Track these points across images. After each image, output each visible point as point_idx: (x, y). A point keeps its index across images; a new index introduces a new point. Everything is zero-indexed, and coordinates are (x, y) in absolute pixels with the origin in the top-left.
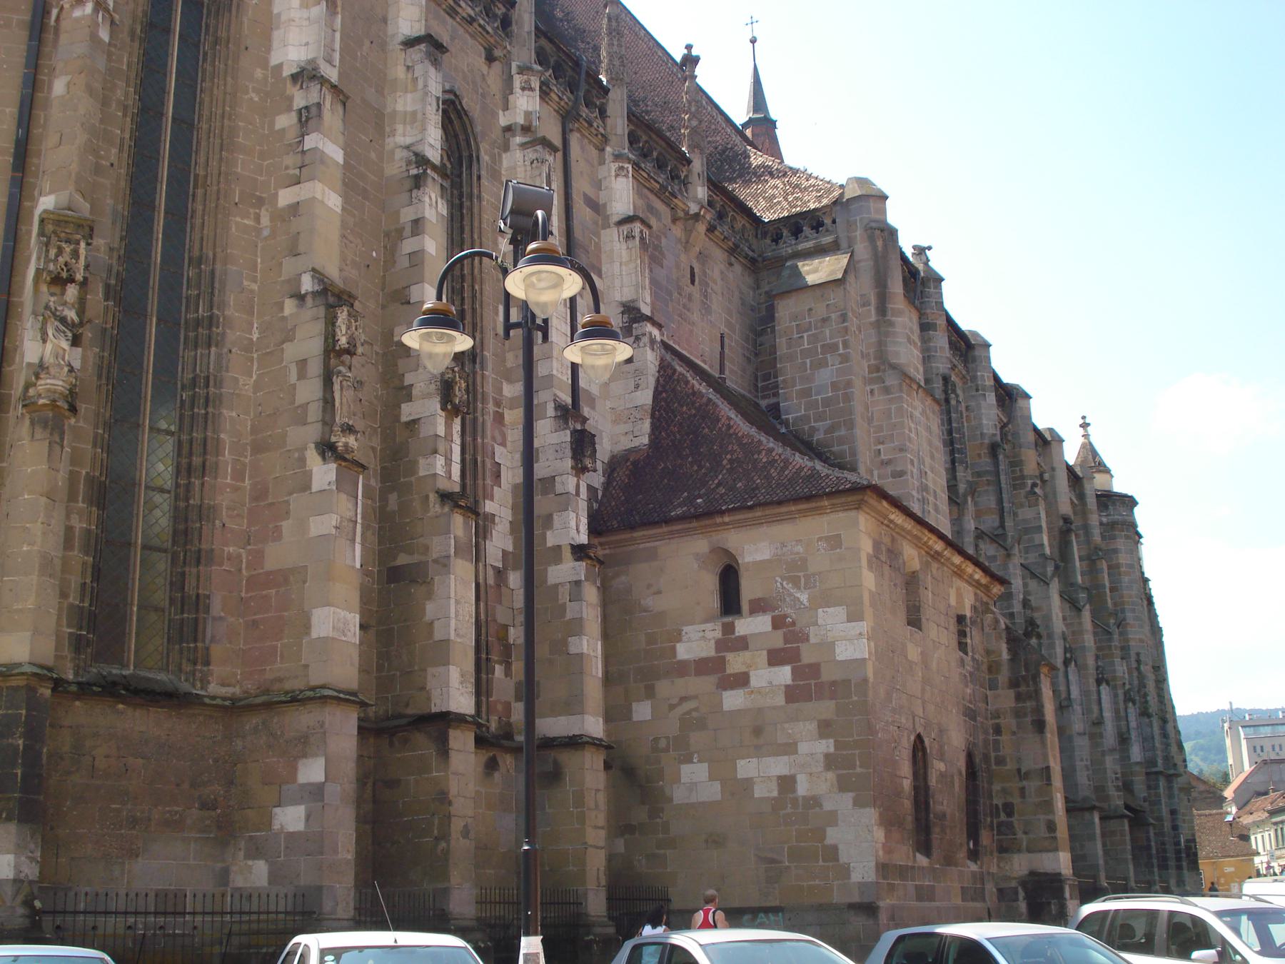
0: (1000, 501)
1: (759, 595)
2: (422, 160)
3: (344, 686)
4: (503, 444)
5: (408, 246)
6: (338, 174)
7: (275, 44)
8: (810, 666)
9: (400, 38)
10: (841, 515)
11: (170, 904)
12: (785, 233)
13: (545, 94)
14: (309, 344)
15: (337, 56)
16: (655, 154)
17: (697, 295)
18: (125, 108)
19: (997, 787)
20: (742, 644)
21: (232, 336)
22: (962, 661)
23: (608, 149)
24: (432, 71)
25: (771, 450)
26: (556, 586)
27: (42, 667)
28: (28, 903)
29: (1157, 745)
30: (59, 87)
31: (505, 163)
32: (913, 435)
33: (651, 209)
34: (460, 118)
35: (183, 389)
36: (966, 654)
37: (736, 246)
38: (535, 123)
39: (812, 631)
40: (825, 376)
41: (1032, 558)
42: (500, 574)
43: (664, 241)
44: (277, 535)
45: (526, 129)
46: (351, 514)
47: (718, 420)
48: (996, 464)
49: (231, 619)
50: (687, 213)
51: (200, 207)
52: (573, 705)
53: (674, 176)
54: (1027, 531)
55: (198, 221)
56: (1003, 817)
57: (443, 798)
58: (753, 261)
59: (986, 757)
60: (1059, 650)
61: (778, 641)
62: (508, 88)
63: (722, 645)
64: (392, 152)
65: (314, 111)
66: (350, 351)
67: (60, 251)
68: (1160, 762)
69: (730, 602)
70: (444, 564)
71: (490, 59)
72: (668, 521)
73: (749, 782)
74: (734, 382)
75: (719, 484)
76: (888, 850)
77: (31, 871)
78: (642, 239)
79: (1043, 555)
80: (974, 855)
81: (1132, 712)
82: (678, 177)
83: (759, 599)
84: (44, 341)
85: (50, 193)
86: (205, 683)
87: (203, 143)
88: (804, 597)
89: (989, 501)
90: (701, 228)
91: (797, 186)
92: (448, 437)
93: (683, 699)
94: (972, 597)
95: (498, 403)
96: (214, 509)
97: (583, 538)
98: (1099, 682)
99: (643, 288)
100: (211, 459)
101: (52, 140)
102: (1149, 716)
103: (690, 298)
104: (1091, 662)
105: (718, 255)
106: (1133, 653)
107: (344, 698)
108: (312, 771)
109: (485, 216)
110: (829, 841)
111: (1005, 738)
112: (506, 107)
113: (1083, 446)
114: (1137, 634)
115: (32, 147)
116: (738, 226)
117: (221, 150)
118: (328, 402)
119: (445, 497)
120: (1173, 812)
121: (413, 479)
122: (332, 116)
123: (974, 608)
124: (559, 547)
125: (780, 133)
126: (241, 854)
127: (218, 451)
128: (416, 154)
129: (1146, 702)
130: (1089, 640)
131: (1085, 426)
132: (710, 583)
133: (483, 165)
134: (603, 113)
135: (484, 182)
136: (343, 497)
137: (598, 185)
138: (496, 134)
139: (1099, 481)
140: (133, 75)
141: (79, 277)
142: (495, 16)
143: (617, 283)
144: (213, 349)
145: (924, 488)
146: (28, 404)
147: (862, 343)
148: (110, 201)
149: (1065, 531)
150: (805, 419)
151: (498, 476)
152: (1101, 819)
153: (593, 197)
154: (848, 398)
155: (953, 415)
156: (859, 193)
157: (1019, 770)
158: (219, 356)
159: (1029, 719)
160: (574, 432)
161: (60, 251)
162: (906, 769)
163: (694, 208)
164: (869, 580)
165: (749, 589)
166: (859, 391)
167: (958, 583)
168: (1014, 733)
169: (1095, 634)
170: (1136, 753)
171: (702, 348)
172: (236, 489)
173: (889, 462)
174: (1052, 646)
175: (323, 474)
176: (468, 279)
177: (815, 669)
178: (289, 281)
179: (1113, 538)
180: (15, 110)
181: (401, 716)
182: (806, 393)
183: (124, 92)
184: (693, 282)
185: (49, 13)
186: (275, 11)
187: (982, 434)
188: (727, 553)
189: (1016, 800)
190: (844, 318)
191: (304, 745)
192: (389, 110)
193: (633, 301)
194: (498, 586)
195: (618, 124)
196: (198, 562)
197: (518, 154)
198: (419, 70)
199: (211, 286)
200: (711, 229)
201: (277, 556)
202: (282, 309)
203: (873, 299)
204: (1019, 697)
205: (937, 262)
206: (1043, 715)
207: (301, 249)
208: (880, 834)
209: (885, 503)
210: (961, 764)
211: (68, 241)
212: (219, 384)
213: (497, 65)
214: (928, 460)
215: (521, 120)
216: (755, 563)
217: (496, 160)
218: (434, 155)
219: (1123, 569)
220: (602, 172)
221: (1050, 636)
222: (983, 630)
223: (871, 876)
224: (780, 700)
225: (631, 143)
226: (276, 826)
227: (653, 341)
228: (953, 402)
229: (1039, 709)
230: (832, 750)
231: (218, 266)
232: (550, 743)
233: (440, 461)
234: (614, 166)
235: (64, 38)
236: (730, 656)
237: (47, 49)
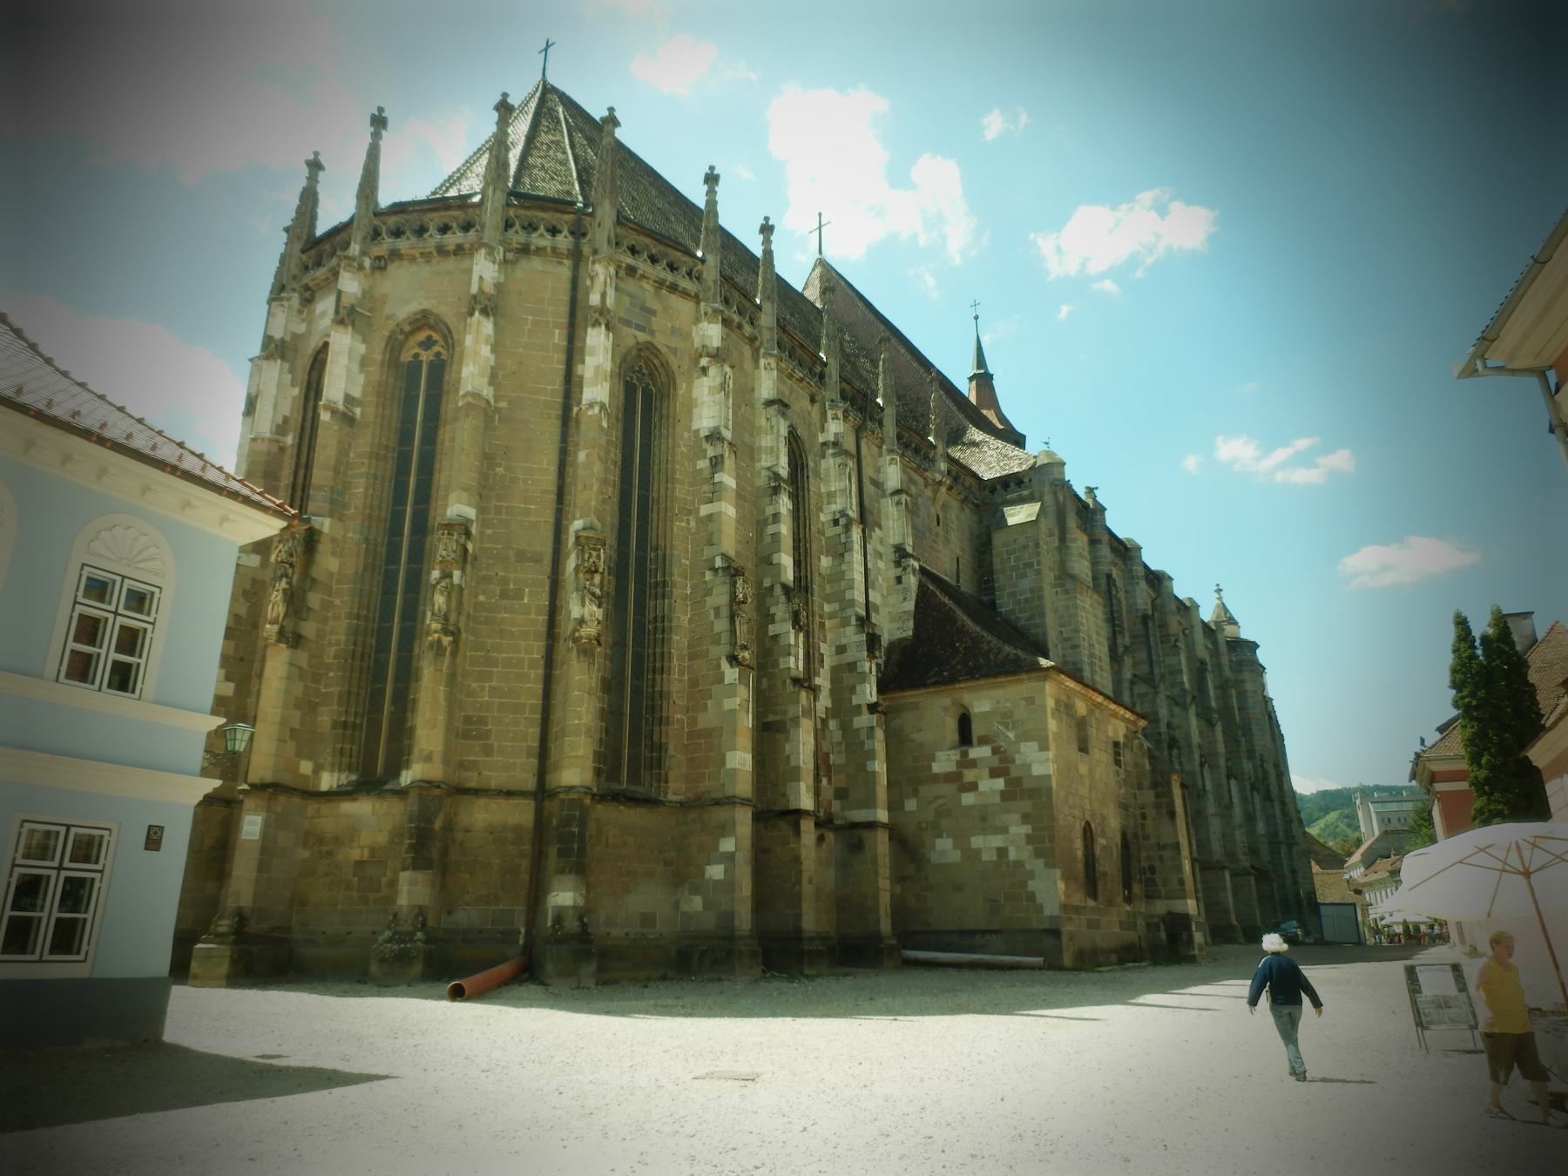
0: (1150, 655)
1: (983, 733)
2: (777, 476)
3: (744, 796)
4: (825, 642)
5: (771, 529)
6: (732, 495)
7: (695, 417)
8: (1015, 778)
9: (763, 401)
10: (1035, 684)
11: (647, 919)
12: (999, 487)
13: (845, 418)
14: (720, 597)
15: (731, 422)
16: (913, 445)
17: (941, 533)
18: (615, 463)
19: (1143, 855)
20: (973, 764)
21: (677, 592)
22: (1118, 772)
23: (884, 447)
24: (782, 421)
25: (990, 642)
26: (858, 730)
27: (586, 788)
28: (581, 918)
29: (1279, 821)
30: (582, 456)
31: (823, 466)
32: (1084, 621)
33: (911, 480)
34: (796, 441)
35: (649, 622)
36: (1120, 767)
37: (966, 497)
38: (841, 440)
39: (1017, 756)
40: (1026, 584)
41: (1176, 692)
42: (824, 722)
43: (920, 500)
44: (705, 708)
45: (835, 444)
46: (746, 697)
47: (956, 621)
48: (1147, 629)
49: (679, 756)
50: (934, 480)
51: (655, 517)
52: (870, 803)
53: (926, 457)
54: (1171, 673)
55: (655, 524)
56: (1148, 875)
57: (797, 860)
58: (977, 506)
59: (1136, 835)
60: (1197, 756)
61: (996, 763)
63: (961, 764)
64: (759, 472)
65: (719, 460)
66: (743, 602)
67: (590, 557)
68: (1281, 834)
69: (965, 735)
70: (796, 721)
71: (813, 400)
72: (925, 685)
73: (978, 852)
74: (966, 586)
75: (957, 664)
76: (1067, 896)
77: (581, 902)
78: (906, 504)
79: (1184, 690)
80: (1128, 900)
81: (1257, 799)
82: (928, 458)
83: (984, 736)
84: (583, 606)
85: (581, 518)
86: (666, 793)
87: (656, 478)
88: (1011, 735)
89: (1143, 655)
90: (943, 489)
91: (1006, 456)
92: (797, 645)
93: (937, 798)
94: (1124, 729)
95: (821, 617)
96: (669, 693)
97: (874, 699)
98: (1229, 777)
99: (908, 535)
100: (666, 664)
101: (580, 487)
102: (1272, 801)
103: (937, 534)
104: (1222, 762)
105: (955, 504)
106: (1258, 754)
107: (745, 802)
108: (728, 845)
109: (812, 501)
110: (1029, 889)
111: (1149, 822)
112: (823, 430)
113: (1218, 606)
114: (1261, 741)
115: (566, 490)
116: (967, 484)
117: (667, 482)
118: (733, 631)
119: (796, 681)
120: (1294, 872)
121: (776, 670)
122: (729, 462)
123: (1126, 736)
124: (860, 705)
125: (995, 382)
126: (687, 892)
127: (670, 660)
128: (774, 473)
129: (1269, 790)
130: (1221, 747)
131: (1219, 591)
132: (951, 724)
133: (810, 468)
134: (881, 423)
135: (811, 480)
136: (742, 687)
137: (878, 470)
138: (817, 448)
139: (1229, 630)
140: (618, 443)
141: (601, 570)
142: (815, 374)
143: (891, 533)
144: (666, 601)
145: (1092, 655)
146: (576, 640)
147: (1048, 560)
148: (609, 519)
149: (1200, 670)
150: (1013, 611)
151: (822, 661)
152: (1231, 876)
153: (874, 477)
154: (1041, 598)
155: (1114, 601)
156: (1046, 462)
157: (1158, 844)
158: (670, 604)
159: (1164, 810)
160: (868, 634)
161: (590, 557)
162: (1079, 844)
163: (938, 477)
164: (1052, 725)
165: (977, 729)
166: (1049, 593)
167: (1113, 720)
168: (1154, 819)
169: (1225, 742)
170: (1261, 828)
171: (944, 567)
172: (680, 681)
173: (1066, 640)
174: (1191, 753)
175: (731, 674)
176: (803, 540)
177: (1018, 781)
178: (707, 560)
179: (1241, 672)
180: (556, 468)
181: (772, 811)
182: (1013, 594)
183: (616, 454)
184: (938, 524)
185: (571, 409)
186: (694, 396)
187: (1137, 610)
188: (963, 706)
189: (1157, 864)
190: (1037, 545)
191: (725, 829)
192: (757, 445)
193: (903, 544)
194: (823, 729)
195: (890, 428)
196: (661, 724)
197: (831, 461)
198: (774, 420)
199: (664, 563)
200: (950, 488)
201: (705, 720)
202: (704, 577)
203: (1056, 532)
204: (1158, 795)
205: (1102, 498)
206: (1174, 807)
207: (714, 541)
208: (1061, 885)
209: (1062, 676)
210: (1118, 839)
211: (594, 549)
212: (670, 620)
213: (817, 406)
214: (1095, 636)
215: (832, 439)
216: (981, 713)
217: (817, 464)
218: (784, 472)
219: (1249, 694)
220: (881, 462)
221: (1190, 746)
222: (1132, 750)
223: (1056, 912)
224: (997, 799)
225: (898, 439)
226: (707, 876)
227: (914, 570)
228: (1114, 592)
229: (1171, 804)
230: (1030, 831)
231: (668, 552)
232: (855, 826)
233: (792, 659)
234: (888, 458)
235: (583, 427)
236: (966, 772)
237: (572, 431)
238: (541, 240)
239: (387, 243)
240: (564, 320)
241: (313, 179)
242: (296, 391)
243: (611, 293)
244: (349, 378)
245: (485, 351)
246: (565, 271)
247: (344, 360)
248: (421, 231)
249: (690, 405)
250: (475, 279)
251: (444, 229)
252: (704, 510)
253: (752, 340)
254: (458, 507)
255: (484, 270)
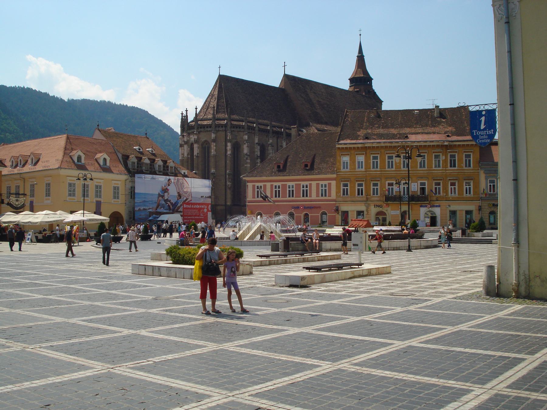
2: (258, 156)
30: (228, 162)
45: (271, 144)
62: (269, 140)
71: (267, 137)
122: (249, 158)
137: (282, 143)
218: (259, 155)
238: (221, 129)
239: (200, 130)
240: (225, 141)
241: (187, 113)
242: (189, 149)
243: (231, 136)
244: (197, 151)
245: (215, 148)
246: (224, 133)
247: (196, 149)
248: (204, 127)
249: (243, 148)
250: (212, 137)
251: (207, 127)
252: (245, 165)
253: (254, 133)
254: (213, 171)
255: (213, 136)
